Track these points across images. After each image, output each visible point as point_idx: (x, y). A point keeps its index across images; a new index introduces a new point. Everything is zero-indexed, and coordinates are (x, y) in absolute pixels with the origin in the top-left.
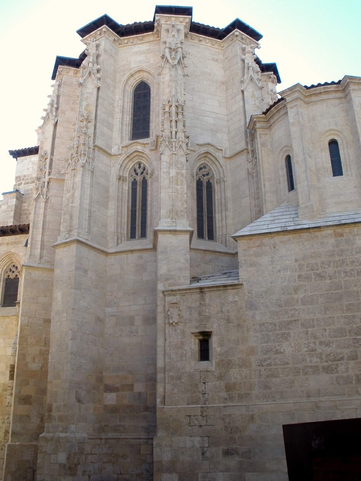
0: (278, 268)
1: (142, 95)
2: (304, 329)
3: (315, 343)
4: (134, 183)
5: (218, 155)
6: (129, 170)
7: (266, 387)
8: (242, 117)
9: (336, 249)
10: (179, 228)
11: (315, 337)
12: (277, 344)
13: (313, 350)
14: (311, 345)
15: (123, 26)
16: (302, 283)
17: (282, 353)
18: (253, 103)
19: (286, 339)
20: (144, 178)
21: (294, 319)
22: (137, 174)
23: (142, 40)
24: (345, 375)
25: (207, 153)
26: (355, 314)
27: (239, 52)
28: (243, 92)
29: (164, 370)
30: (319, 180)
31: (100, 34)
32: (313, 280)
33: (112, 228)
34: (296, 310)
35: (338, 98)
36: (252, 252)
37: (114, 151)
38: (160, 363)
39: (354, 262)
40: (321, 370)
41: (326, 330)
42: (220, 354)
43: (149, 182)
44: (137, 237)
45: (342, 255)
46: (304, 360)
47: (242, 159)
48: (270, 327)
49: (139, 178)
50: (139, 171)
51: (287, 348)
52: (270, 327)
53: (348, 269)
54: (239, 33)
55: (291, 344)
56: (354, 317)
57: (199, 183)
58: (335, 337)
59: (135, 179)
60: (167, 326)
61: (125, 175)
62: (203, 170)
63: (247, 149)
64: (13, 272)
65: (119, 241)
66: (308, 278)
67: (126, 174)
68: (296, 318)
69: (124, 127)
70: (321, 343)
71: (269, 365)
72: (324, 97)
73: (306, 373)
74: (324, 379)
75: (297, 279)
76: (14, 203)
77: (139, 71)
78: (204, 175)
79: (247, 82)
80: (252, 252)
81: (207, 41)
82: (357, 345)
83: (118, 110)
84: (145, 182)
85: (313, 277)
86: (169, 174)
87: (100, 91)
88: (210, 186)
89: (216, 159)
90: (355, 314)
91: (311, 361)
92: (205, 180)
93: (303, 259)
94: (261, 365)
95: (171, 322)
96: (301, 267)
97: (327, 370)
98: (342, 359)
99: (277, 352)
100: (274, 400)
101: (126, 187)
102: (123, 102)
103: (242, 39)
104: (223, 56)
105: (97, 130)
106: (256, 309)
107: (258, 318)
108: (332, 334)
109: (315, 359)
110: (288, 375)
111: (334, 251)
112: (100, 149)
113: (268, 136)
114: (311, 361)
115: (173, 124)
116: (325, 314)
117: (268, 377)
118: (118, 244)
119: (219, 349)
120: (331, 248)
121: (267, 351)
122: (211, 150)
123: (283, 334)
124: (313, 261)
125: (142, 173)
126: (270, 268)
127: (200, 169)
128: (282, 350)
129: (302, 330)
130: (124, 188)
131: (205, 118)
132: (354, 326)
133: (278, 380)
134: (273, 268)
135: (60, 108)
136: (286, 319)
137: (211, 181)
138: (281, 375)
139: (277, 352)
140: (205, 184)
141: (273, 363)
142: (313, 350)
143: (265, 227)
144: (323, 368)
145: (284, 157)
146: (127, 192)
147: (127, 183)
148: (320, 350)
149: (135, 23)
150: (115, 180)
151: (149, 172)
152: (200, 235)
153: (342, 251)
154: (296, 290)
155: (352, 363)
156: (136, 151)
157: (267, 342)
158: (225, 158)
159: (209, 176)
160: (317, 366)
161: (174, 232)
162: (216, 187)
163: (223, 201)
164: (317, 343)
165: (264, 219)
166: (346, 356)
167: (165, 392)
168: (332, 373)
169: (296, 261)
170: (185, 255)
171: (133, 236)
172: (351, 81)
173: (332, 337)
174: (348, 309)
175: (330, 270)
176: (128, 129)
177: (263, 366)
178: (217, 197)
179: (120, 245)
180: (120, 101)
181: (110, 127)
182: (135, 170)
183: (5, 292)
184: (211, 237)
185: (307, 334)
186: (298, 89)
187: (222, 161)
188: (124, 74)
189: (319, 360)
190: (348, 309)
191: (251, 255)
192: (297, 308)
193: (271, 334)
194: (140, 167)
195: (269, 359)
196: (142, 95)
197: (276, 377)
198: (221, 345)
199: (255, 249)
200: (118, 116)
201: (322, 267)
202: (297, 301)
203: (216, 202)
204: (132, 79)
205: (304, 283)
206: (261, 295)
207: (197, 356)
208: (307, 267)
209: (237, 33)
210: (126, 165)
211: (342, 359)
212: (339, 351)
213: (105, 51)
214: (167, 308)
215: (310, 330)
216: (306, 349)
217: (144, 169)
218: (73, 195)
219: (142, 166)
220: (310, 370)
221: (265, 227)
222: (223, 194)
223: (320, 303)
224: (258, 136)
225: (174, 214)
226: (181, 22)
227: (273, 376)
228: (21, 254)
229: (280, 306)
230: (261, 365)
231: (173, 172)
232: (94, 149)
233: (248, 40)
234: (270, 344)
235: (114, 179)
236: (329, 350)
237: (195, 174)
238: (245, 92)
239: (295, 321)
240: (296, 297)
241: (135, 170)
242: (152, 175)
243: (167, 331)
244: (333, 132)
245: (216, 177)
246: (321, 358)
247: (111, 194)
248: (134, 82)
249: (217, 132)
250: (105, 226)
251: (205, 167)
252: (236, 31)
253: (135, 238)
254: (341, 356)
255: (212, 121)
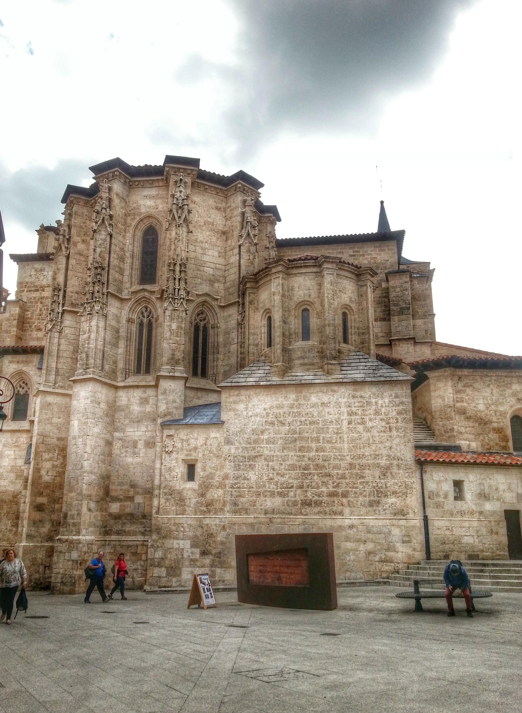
0: (250, 414)
1: (150, 240)
2: (266, 463)
3: (273, 474)
4: (141, 324)
5: (214, 303)
6: (137, 313)
7: (235, 504)
8: (236, 270)
9: (295, 403)
10: (177, 374)
11: (274, 469)
12: (245, 472)
13: (271, 479)
14: (271, 475)
15: (135, 167)
16: (267, 427)
17: (248, 479)
18: (248, 258)
19: (252, 469)
20: (150, 321)
21: (259, 454)
22: (144, 317)
23: (152, 184)
24: (293, 499)
25: (205, 301)
26: (305, 454)
27: (240, 204)
28: (240, 246)
29: (159, 487)
30: (290, 342)
31: (113, 176)
32: (276, 425)
33: (121, 365)
34: (261, 447)
35: (314, 272)
36: (231, 400)
37: (125, 295)
38: (157, 482)
39: (308, 414)
40: (276, 494)
41: (282, 464)
42: (202, 478)
43: (154, 325)
44: (142, 373)
45: (299, 408)
46: (264, 486)
47: (233, 311)
48: (241, 459)
49: (145, 320)
50: (146, 314)
51: (252, 476)
52: (241, 459)
53: (303, 419)
54: (241, 184)
55: (255, 474)
56: (304, 456)
57: (197, 328)
58: (289, 470)
59: (142, 321)
60: (164, 453)
61: (133, 317)
62: (201, 316)
63: (238, 302)
64: (23, 388)
65: (127, 376)
66: (272, 423)
67: (135, 316)
68: (261, 454)
69: (134, 272)
70: (277, 474)
71: (239, 488)
72: (304, 270)
73: (265, 496)
74: (278, 501)
75: (264, 424)
76: (18, 312)
77: (149, 216)
78: (201, 321)
79: (244, 237)
80: (231, 400)
81: (212, 189)
82: (304, 477)
83: (128, 254)
84: (150, 324)
85: (276, 423)
86: (171, 327)
87: (113, 238)
88: (205, 328)
89: (212, 307)
90: (305, 454)
91: (269, 487)
92: (202, 323)
93: (270, 408)
94: (232, 487)
95: (167, 450)
96: (268, 414)
97: (280, 494)
98: (292, 487)
99: (245, 479)
100: (240, 515)
101: (134, 328)
102: (133, 246)
103: (244, 190)
104: (226, 204)
105: (110, 277)
106: (232, 444)
107: (233, 451)
108: (287, 468)
109: (272, 486)
110: (252, 497)
111: (294, 404)
112: (113, 295)
113: (256, 295)
114: (269, 487)
115: (177, 283)
116: (283, 452)
117: (237, 497)
118: (126, 379)
119: (202, 473)
120: (292, 402)
121: (237, 478)
122: (208, 299)
123: (250, 465)
124: (277, 411)
125: (148, 316)
126: (245, 413)
127: (198, 315)
128: (249, 477)
129: (264, 463)
130: (132, 328)
131: (206, 268)
132: (303, 463)
133: (244, 499)
134: (247, 413)
135: (72, 240)
136: (253, 453)
137: (207, 326)
138: (247, 496)
139: (245, 479)
140: (201, 329)
141: (242, 486)
142: (271, 479)
143: (243, 380)
144: (278, 493)
145: (267, 317)
146: (134, 332)
147: (135, 325)
148: (277, 479)
149: (146, 165)
150: (124, 322)
151: (155, 316)
152: (195, 374)
153: (300, 404)
154: (262, 432)
155: (299, 491)
156: (144, 297)
157: (239, 470)
158: (220, 307)
159: (205, 322)
160: (274, 492)
161: (173, 378)
162: (211, 332)
163: (216, 344)
164: (275, 474)
165: (244, 372)
166: (295, 485)
167: (159, 504)
168: (284, 497)
169: (265, 409)
170: (180, 396)
171: (138, 371)
172: (326, 260)
173: (286, 470)
174: (300, 450)
175: (290, 419)
176: (136, 273)
177: (234, 488)
178: (211, 340)
179: (126, 381)
180: (130, 246)
181: (121, 272)
182: (142, 313)
183: (15, 407)
184: (204, 375)
185: (268, 466)
186: (282, 263)
187: (217, 310)
188: (135, 219)
189: (275, 487)
190: (300, 450)
191: (231, 403)
192: (262, 446)
193: (241, 464)
194: (146, 311)
195: (239, 483)
196: (150, 240)
197: (243, 497)
198: (204, 470)
199: (234, 397)
200: (128, 261)
201: (283, 416)
202: (263, 441)
203: (210, 344)
204: (142, 223)
205: (269, 427)
206: (236, 434)
207: (186, 477)
208: (272, 415)
209: (240, 185)
210: (135, 308)
211: (292, 487)
212: (291, 481)
213: (117, 195)
214: (164, 438)
215: (270, 463)
216: (266, 478)
217: (150, 313)
218: (89, 337)
219: (148, 310)
220: (269, 493)
221: (243, 380)
222: (216, 338)
223: (279, 443)
224: (247, 295)
225: (174, 361)
226: (189, 174)
227: (240, 496)
228: (31, 373)
229: (250, 443)
230: (232, 487)
231: (174, 326)
232: (107, 296)
233: (250, 191)
234: (241, 472)
235: (124, 321)
236: (282, 479)
237: (193, 320)
238: (242, 247)
239: (260, 456)
240: (262, 437)
241: (142, 313)
242: (157, 320)
243: (163, 457)
244: (306, 303)
245: (212, 322)
246: (277, 486)
247: (121, 334)
248: (143, 227)
249: (215, 282)
250: (115, 362)
251: (202, 313)
252: (239, 183)
253: (140, 373)
254: (292, 484)
255: (211, 271)
